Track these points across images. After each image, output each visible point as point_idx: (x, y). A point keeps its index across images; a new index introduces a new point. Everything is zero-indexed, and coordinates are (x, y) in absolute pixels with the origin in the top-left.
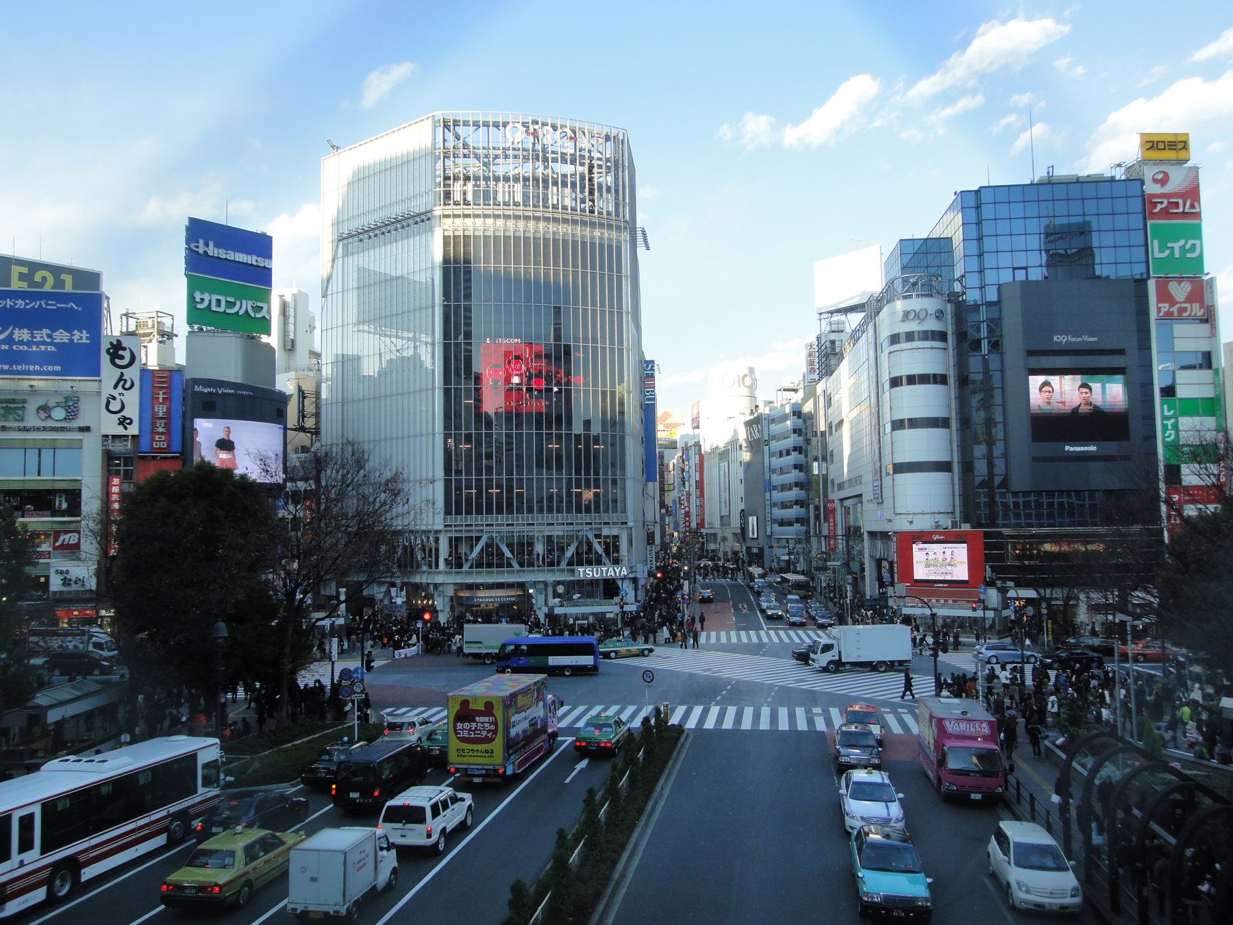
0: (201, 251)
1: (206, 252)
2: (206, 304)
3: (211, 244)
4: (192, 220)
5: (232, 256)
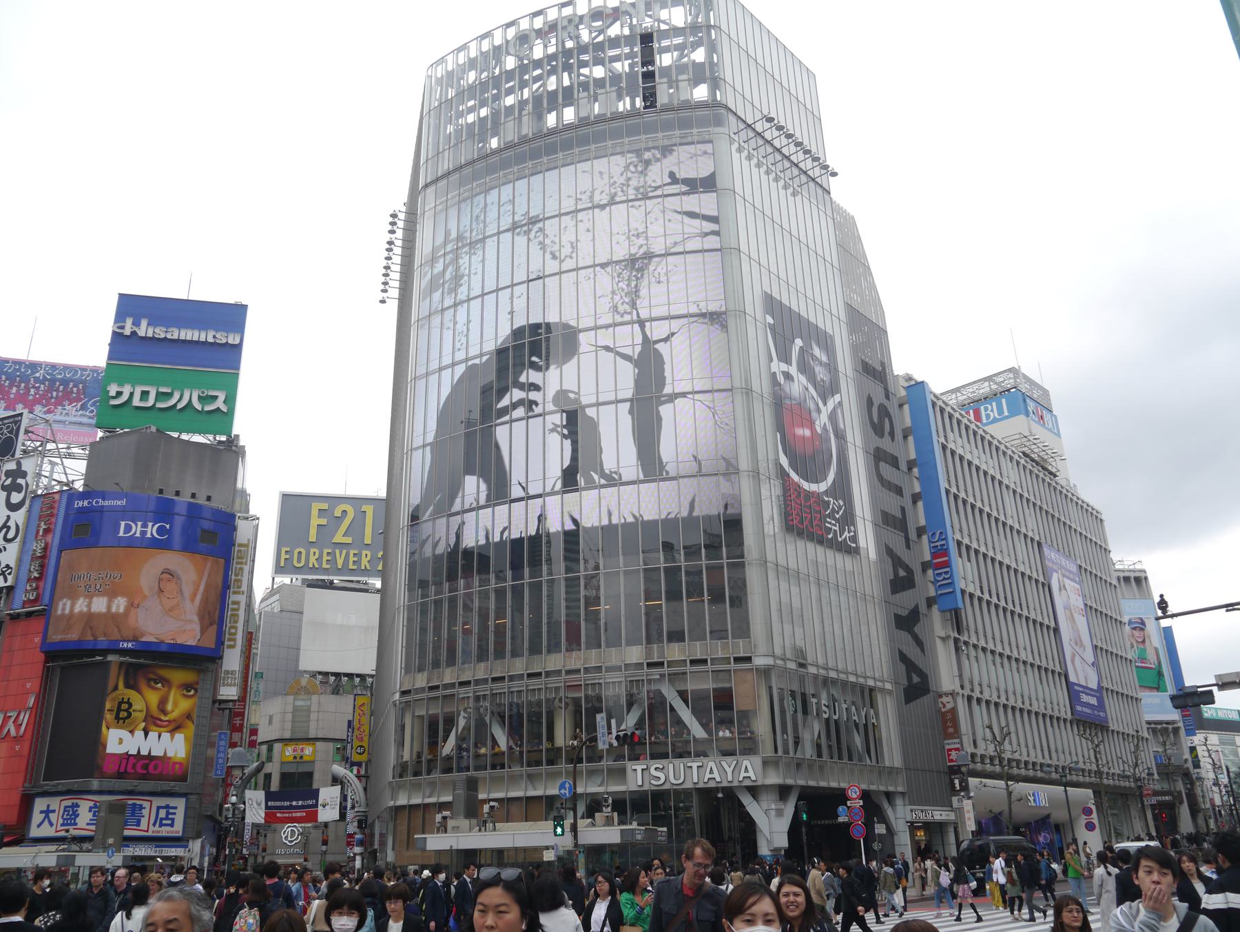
0: (127, 332)
1: (134, 333)
2: (125, 397)
3: (144, 323)
4: (121, 295)
5: (174, 334)
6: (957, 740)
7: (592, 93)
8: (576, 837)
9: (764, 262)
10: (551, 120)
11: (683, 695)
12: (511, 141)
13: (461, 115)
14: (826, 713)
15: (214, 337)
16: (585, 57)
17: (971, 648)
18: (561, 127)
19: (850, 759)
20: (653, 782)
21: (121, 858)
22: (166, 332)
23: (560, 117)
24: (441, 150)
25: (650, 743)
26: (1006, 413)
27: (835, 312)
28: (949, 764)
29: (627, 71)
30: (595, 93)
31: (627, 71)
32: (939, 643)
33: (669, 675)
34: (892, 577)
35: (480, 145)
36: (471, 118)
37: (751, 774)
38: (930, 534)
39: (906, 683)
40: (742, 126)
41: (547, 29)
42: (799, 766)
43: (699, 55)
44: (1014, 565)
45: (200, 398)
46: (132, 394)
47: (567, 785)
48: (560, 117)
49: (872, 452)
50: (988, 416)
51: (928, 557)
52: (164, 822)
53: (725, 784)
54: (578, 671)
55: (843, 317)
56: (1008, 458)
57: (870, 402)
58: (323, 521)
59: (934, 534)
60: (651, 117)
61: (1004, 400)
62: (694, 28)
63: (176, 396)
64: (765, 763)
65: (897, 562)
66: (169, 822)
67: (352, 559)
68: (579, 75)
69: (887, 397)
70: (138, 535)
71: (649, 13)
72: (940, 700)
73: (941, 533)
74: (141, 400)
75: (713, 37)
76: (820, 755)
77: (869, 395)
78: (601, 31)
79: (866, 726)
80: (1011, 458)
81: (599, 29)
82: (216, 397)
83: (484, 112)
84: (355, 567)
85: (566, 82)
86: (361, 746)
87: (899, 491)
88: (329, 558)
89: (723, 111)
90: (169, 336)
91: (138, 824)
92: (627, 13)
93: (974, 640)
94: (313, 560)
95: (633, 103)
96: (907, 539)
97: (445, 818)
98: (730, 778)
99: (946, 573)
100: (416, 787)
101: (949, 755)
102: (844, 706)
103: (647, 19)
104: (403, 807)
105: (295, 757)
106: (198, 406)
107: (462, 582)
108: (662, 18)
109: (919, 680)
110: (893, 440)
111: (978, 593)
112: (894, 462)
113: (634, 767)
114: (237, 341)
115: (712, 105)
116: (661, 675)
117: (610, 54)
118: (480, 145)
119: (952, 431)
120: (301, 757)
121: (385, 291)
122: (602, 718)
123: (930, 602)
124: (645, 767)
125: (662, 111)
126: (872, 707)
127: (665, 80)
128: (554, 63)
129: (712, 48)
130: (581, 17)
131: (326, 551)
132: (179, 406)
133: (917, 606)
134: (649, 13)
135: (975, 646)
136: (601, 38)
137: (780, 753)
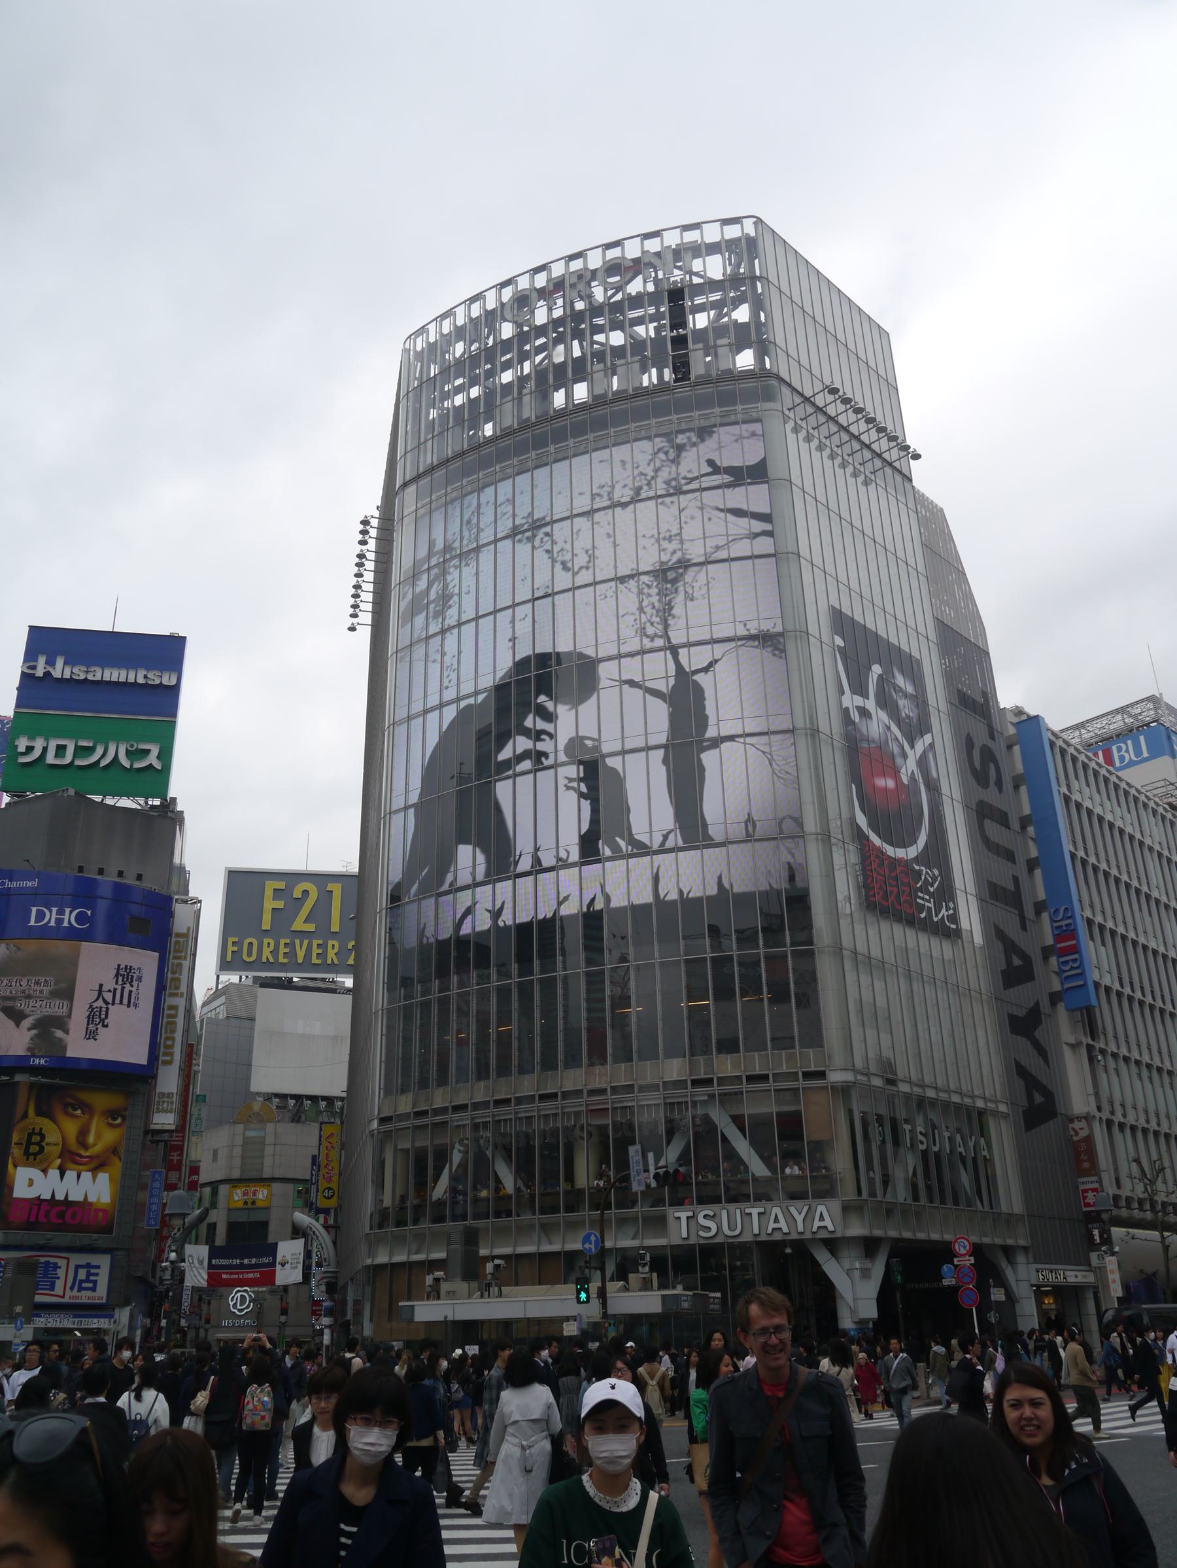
0: (40, 673)
1: (47, 674)
2: (37, 753)
3: (60, 662)
4: (33, 630)
5: (97, 674)
6: (1095, 1178)
7: (609, 364)
8: (604, 1305)
9: (830, 569)
10: (559, 399)
11: (738, 1121)
12: (510, 427)
13: (447, 396)
14: (922, 1143)
15: (145, 677)
16: (600, 321)
17: (1110, 1059)
18: (571, 407)
19: (956, 1203)
20: (702, 1233)
21: (32, 1330)
22: (87, 672)
23: (569, 396)
24: (422, 440)
25: (696, 1183)
26: (1145, 754)
27: (921, 629)
28: (1085, 1209)
29: (653, 336)
30: (612, 364)
31: (653, 336)
32: (1067, 1052)
33: (719, 1095)
34: (1004, 967)
35: (471, 433)
36: (459, 400)
37: (828, 1223)
38: (1052, 911)
39: (1025, 1103)
40: (798, 400)
41: (551, 287)
42: (889, 1212)
43: (742, 314)
44: (1162, 949)
45: (128, 753)
46: (45, 750)
47: (593, 1238)
48: (569, 396)
49: (974, 807)
50: (1122, 758)
51: (1049, 940)
52: (84, 1285)
53: (794, 1236)
54: (602, 1091)
55: (932, 636)
56: (1150, 811)
57: (969, 743)
58: (280, 904)
59: (1057, 911)
60: (683, 392)
61: (1142, 738)
62: (734, 280)
63: (100, 751)
64: (846, 1209)
65: (1010, 947)
66: (90, 1285)
67: (315, 951)
68: (593, 342)
69: (992, 737)
70: (53, 923)
71: (678, 264)
72: (1071, 1126)
73: (1066, 909)
74: (57, 756)
75: (760, 291)
76: (916, 1198)
77: (968, 734)
78: (619, 288)
79: (974, 1160)
80: (1154, 812)
81: (615, 285)
82: (147, 752)
83: (475, 392)
84: (319, 962)
85: (577, 353)
86: (329, 1189)
87: (1010, 856)
88: (287, 950)
89: (774, 382)
90: (90, 677)
91: (52, 1288)
92: (651, 265)
93: (1113, 1048)
94: (266, 952)
95: (660, 376)
96: (1023, 918)
97: (437, 1280)
98: (800, 1228)
99: (1075, 960)
100: (400, 1241)
101: (1085, 1198)
102: (947, 1134)
103: (676, 272)
104: (382, 1267)
105: (246, 1203)
106: (126, 763)
107: (455, 979)
108: (695, 270)
109: (1043, 1099)
110: (1000, 790)
111: (1117, 986)
112: (1003, 819)
113: (677, 1215)
114: (173, 682)
115: (759, 374)
116: (709, 1096)
117: (630, 316)
118: (471, 433)
119: (1077, 778)
120: (253, 1203)
121: (354, 616)
122: (637, 1151)
123: (1055, 998)
124: (691, 1214)
125: (697, 384)
126: (982, 1135)
127: (700, 346)
128: (561, 329)
129: (758, 305)
130: (594, 272)
131: (282, 941)
132: (103, 763)
133: (1037, 1003)
134: (678, 264)
135: (1115, 1056)
136: (619, 297)
137: (865, 1195)
